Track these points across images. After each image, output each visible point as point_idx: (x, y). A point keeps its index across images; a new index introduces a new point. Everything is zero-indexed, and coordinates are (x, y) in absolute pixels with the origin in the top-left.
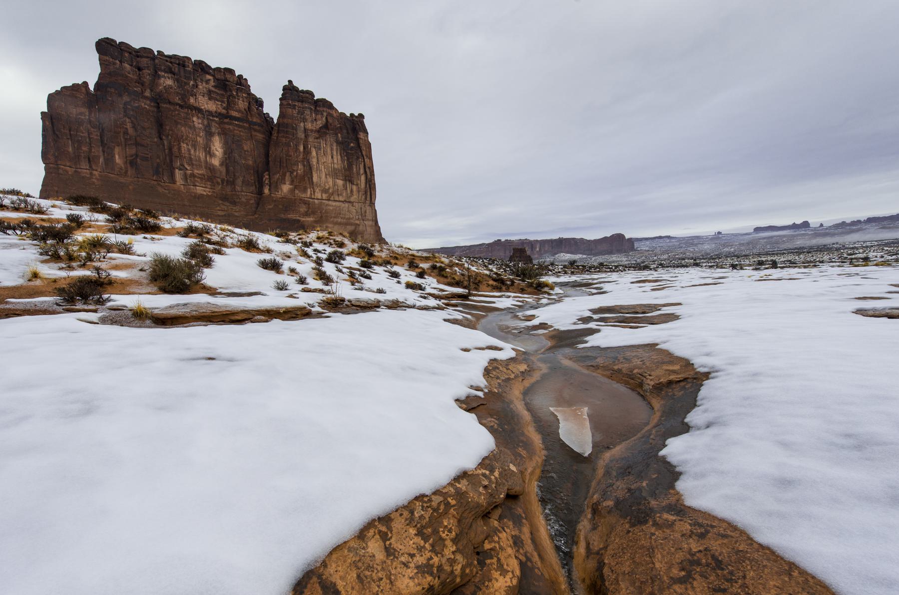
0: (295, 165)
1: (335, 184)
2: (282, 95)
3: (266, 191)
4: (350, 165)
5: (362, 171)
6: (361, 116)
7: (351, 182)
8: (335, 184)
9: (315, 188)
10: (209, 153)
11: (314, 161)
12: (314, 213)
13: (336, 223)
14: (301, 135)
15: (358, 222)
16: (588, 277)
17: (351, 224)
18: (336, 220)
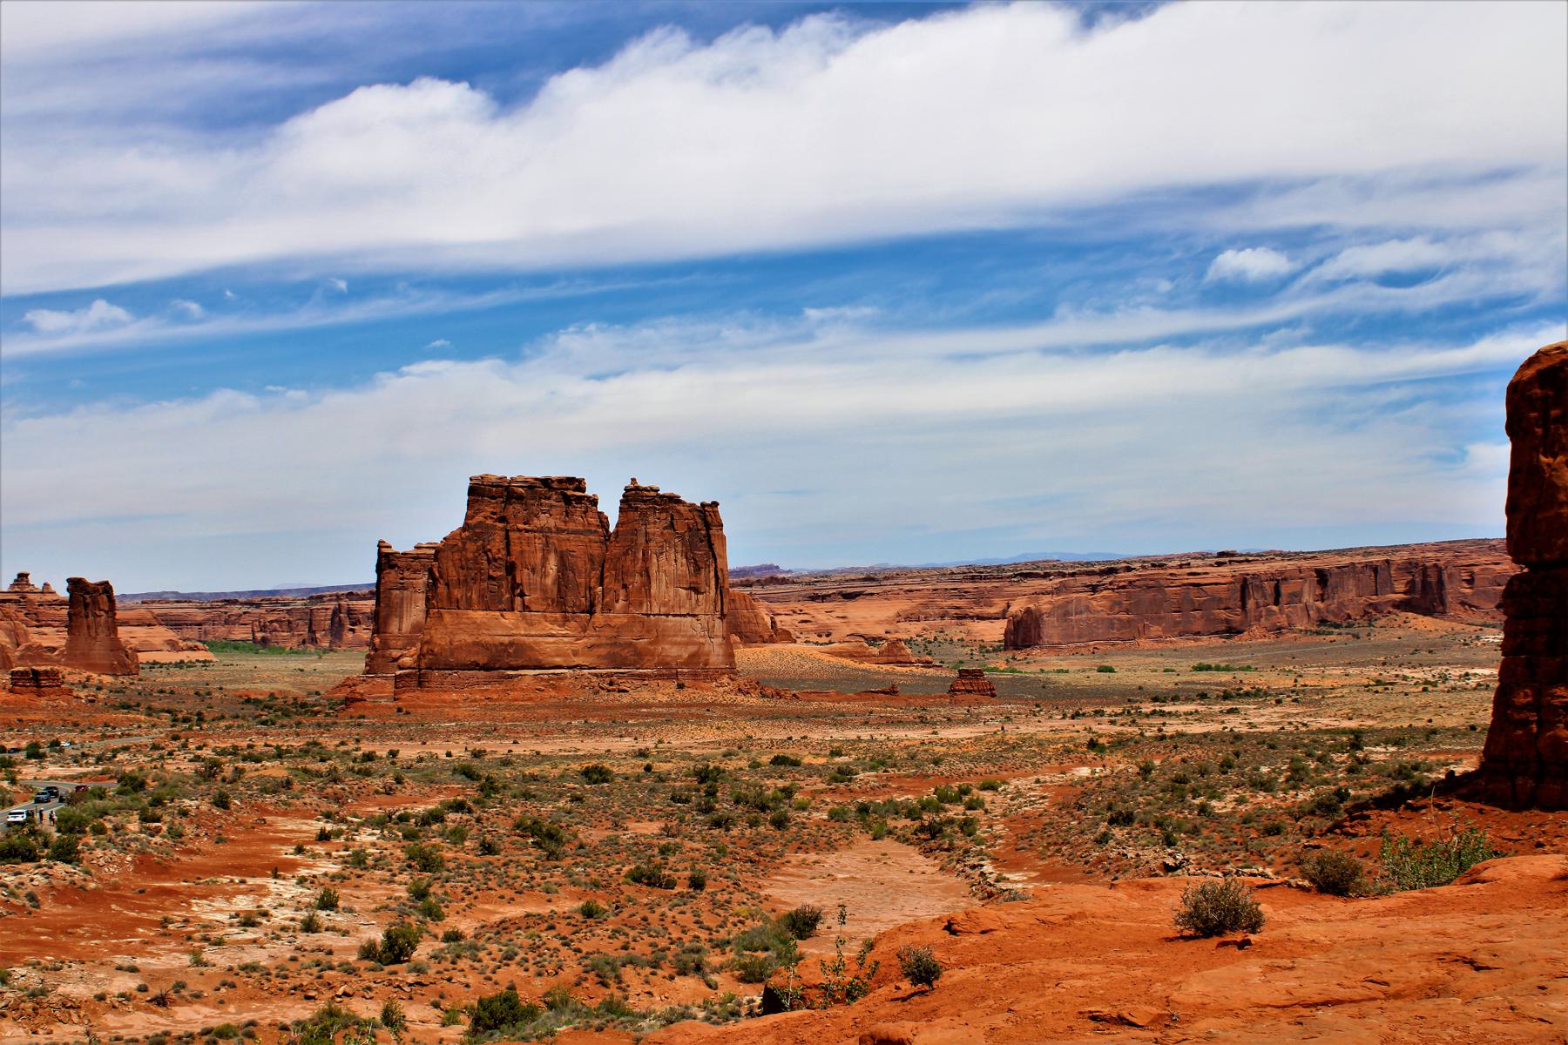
0: (631, 576)
1: (676, 594)
2: (624, 496)
3: (598, 608)
4: (698, 570)
5: (712, 574)
6: (715, 504)
7: (697, 591)
8: (676, 594)
9: (653, 600)
10: (545, 575)
11: (654, 569)
12: (648, 631)
13: (676, 644)
14: (642, 540)
15: (702, 640)
16: (916, 735)
17: (694, 644)
18: (675, 639)
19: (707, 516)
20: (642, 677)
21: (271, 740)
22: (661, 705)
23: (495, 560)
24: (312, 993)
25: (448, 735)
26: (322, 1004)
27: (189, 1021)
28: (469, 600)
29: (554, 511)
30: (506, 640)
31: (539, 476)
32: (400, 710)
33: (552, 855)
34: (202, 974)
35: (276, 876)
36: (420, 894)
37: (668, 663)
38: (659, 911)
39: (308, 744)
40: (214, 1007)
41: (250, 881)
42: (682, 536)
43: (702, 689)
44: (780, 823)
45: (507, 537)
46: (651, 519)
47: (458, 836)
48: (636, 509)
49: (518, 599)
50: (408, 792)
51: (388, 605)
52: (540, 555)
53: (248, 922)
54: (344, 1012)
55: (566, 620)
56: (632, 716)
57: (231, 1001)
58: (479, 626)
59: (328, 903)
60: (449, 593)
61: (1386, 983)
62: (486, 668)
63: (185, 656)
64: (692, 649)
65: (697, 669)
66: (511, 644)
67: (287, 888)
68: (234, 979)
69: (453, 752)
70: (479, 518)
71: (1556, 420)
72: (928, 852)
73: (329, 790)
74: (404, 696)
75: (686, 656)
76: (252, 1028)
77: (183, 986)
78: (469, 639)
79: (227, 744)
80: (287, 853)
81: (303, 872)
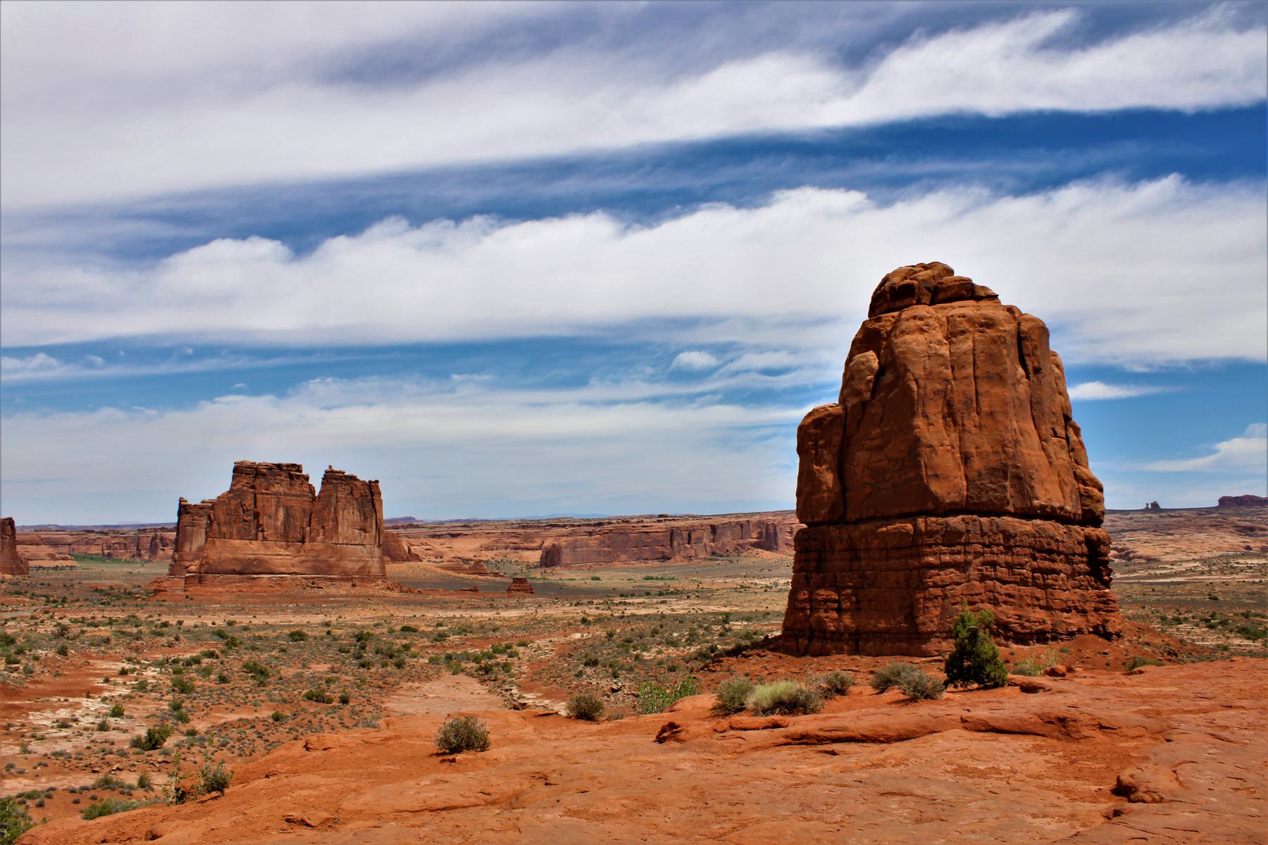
1: (353, 532)
3: (307, 540)
4: (366, 519)
5: (374, 521)
7: (365, 531)
8: (353, 532)
10: (276, 520)
11: (340, 519)
12: (336, 554)
14: (334, 501)
16: (487, 614)
17: (362, 561)
19: (372, 489)
20: (331, 579)
21: (107, 614)
22: (342, 596)
23: (248, 510)
24: (97, 769)
25: (215, 612)
26: (101, 776)
27: (13, 789)
28: (231, 533)
29: (283, 483)
30: (253, 557)
31: (275, 463)
32: (187, 597)
33: (261, 684)
34: (26, 759)
35: (88, 697)
36: (176, 707)
37: (346, 572)
38: (319, 716)
39: (129, 616)
40: (32, 779)
41: (71, 700)
42: (357, 499)
43: (366, 587)
44: (399, 665)
45: (255, 497)
46: (340, 489)
47: (207, 672)
48: (331, 483)
49: (260, 534)
50: (183, 645)
51: (184, 536)
52: (274, 508)
53: (63, 725)
54: (115, 780)
55: (288, 546)
56: (325, 602)
57: (43, 775)
58: (236, 549)
59: (117, 713)
60: (220, 529)
61: (489, 794)
62: (240, 573)
63: (59, 563)
64: (361, 564)
65: (364, 576)
66: (255, 559)
67: (94, 704)
68: (47, 761)
69: (216, 622)
70: (239, 486)
71: (821, 447)
72: (483, 682)
73: (133, 644)
74: (191, 589)
75: (357, 568)
76: (51, 792)
77: (12, 766)
78: (231, 556)
79: (79, 616)
80: (99, 682)
81: (107, 694)
